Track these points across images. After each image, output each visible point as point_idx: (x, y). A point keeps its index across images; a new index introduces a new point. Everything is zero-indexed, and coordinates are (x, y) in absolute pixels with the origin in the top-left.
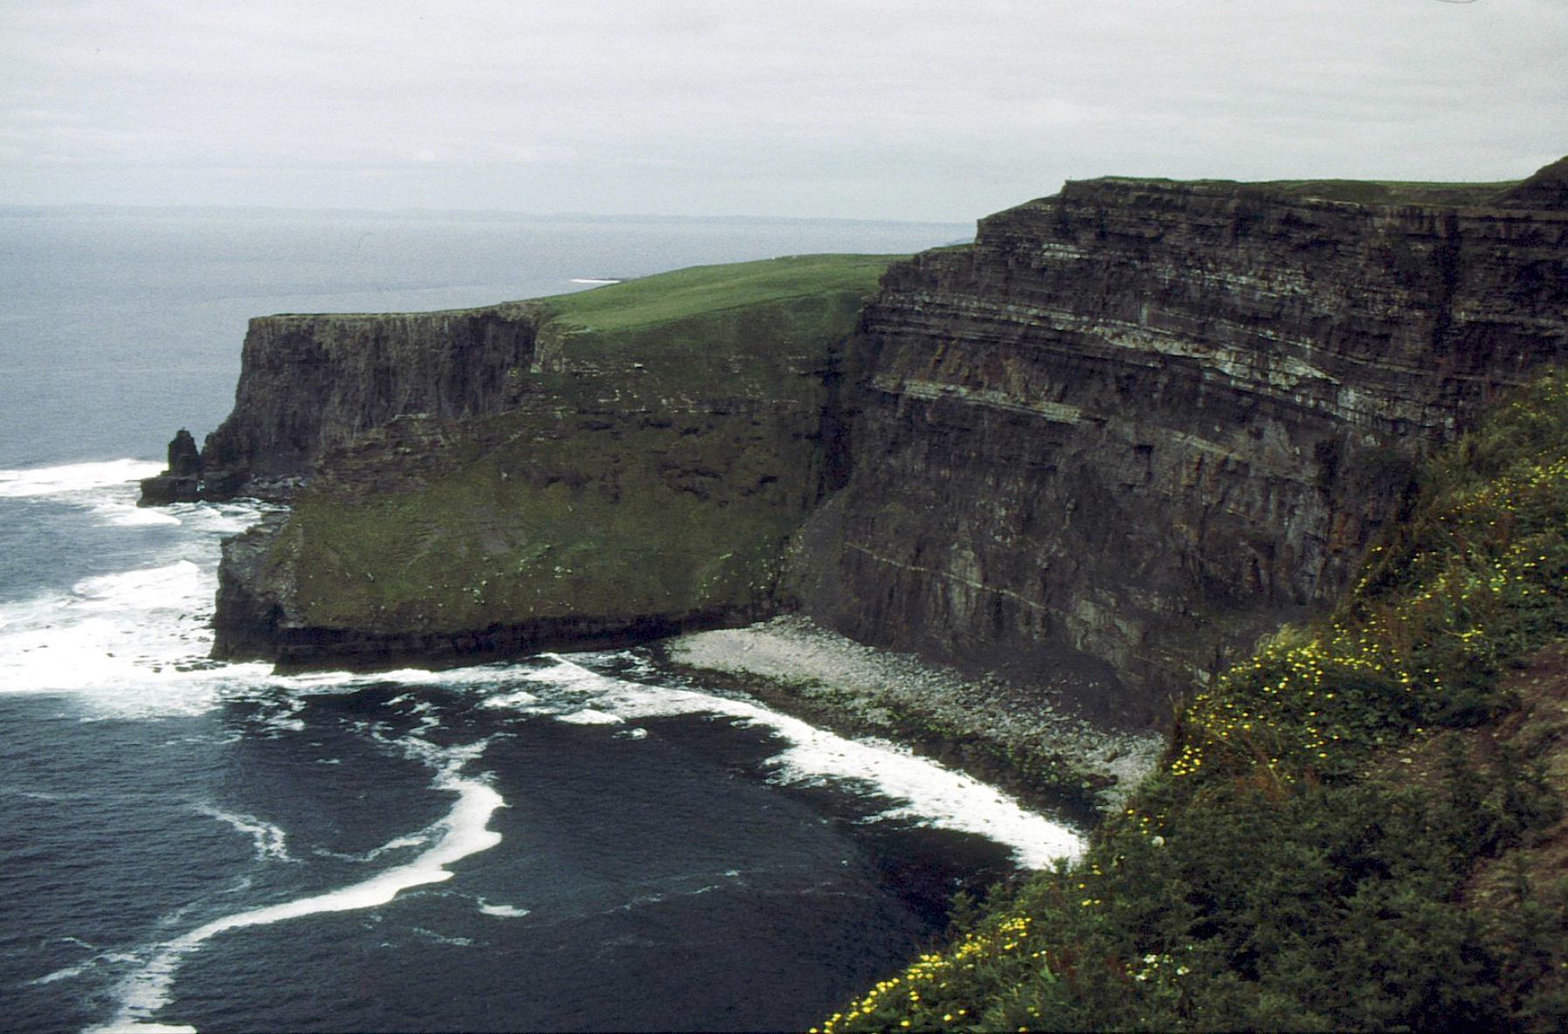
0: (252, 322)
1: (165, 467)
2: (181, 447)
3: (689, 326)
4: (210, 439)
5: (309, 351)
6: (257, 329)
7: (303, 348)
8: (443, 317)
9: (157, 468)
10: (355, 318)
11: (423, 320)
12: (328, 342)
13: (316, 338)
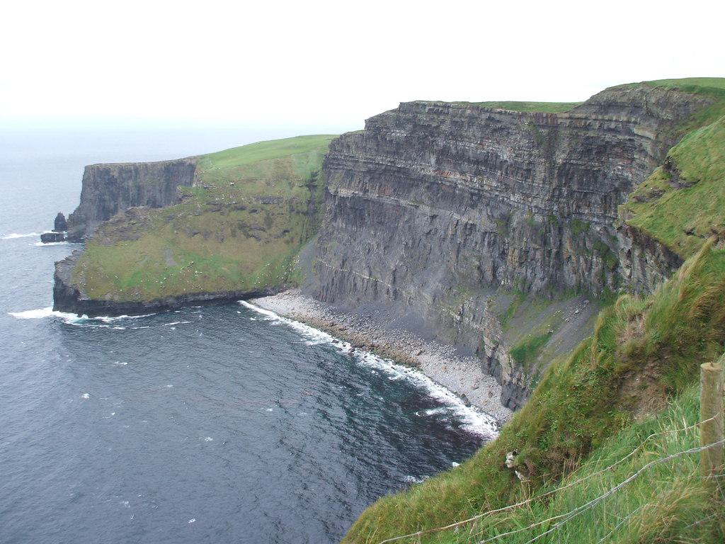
0: (86, 168)
2: (60, 223)
4: (70, 215)
6: (88, 169)
11: (154, 165)
12: (116, 175)
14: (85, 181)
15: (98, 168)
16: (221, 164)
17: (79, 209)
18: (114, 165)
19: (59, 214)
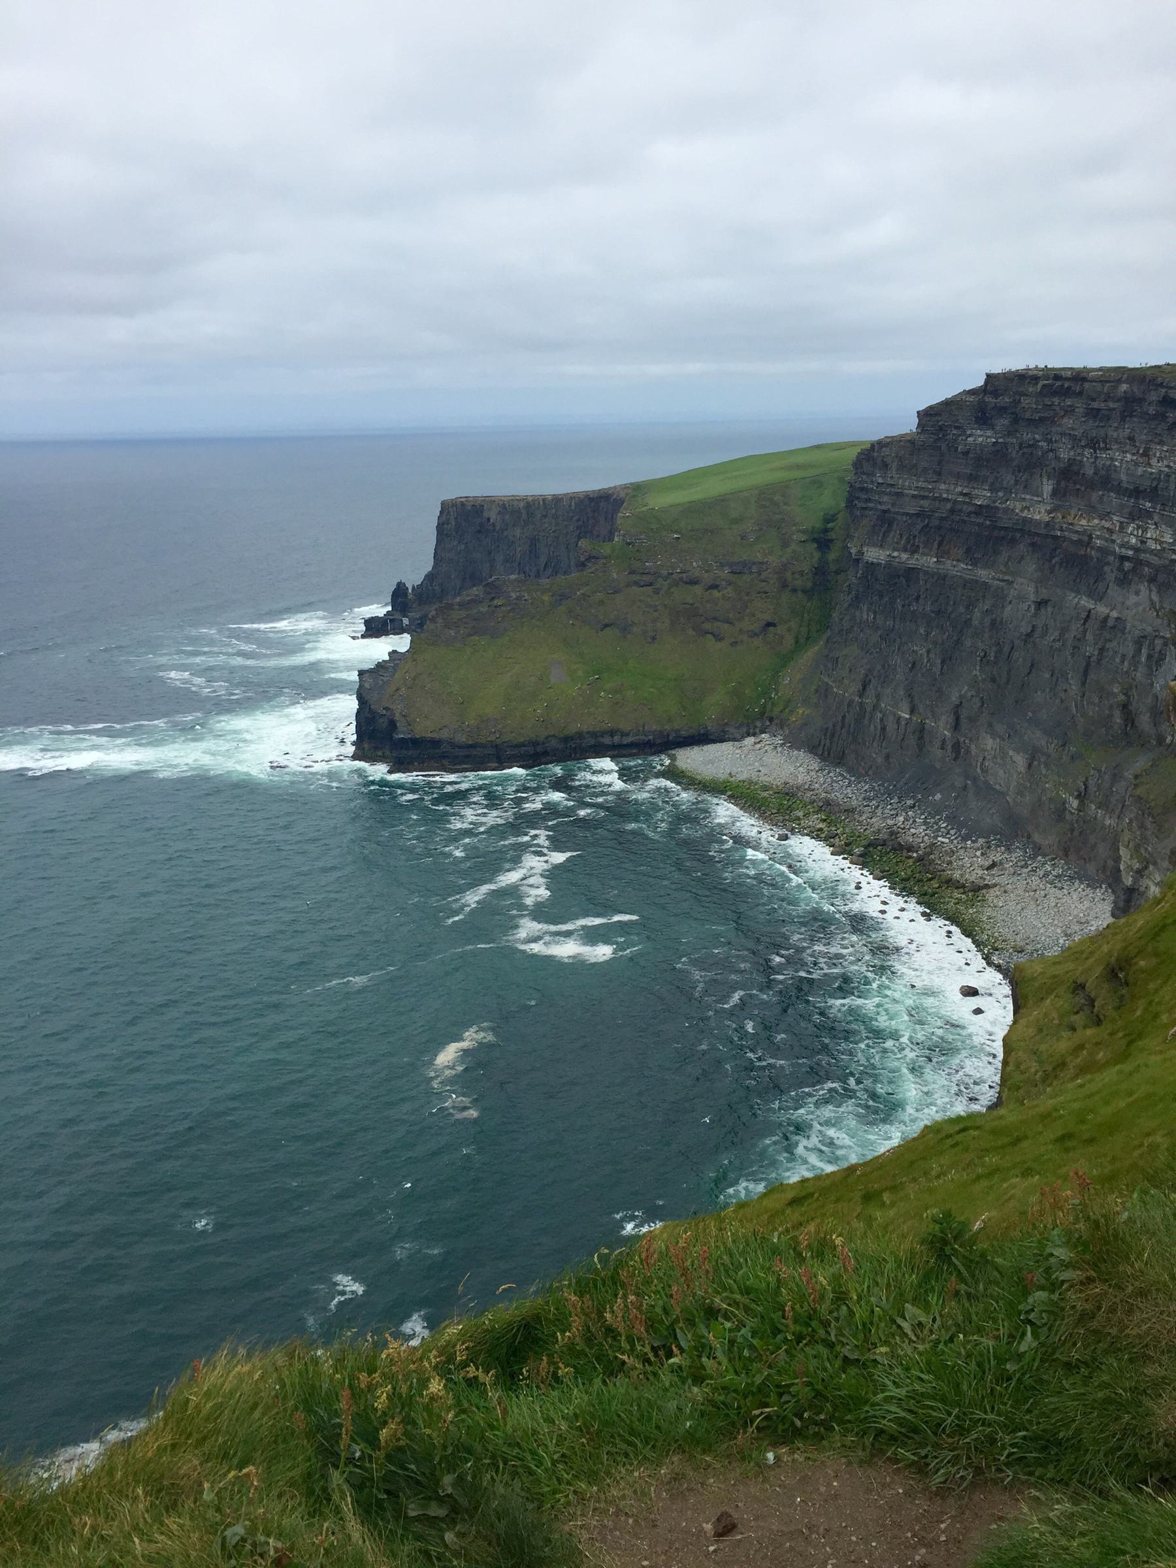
0: (443, 503)
1: (390, 608)
2: (399, 595)
3: (720, 502)
5: (481, 525)
6: (446, 507)
8: (572, 497)
9: (379, 610)
10: (515, 499)
11: (557, 499)
12: (493, 515)
13: (486, 514)
14: (440, 528)
15: (462, 504)
16: (658, 501)
17: (430, 577)
18: (490, 501)
19: (399, 584)
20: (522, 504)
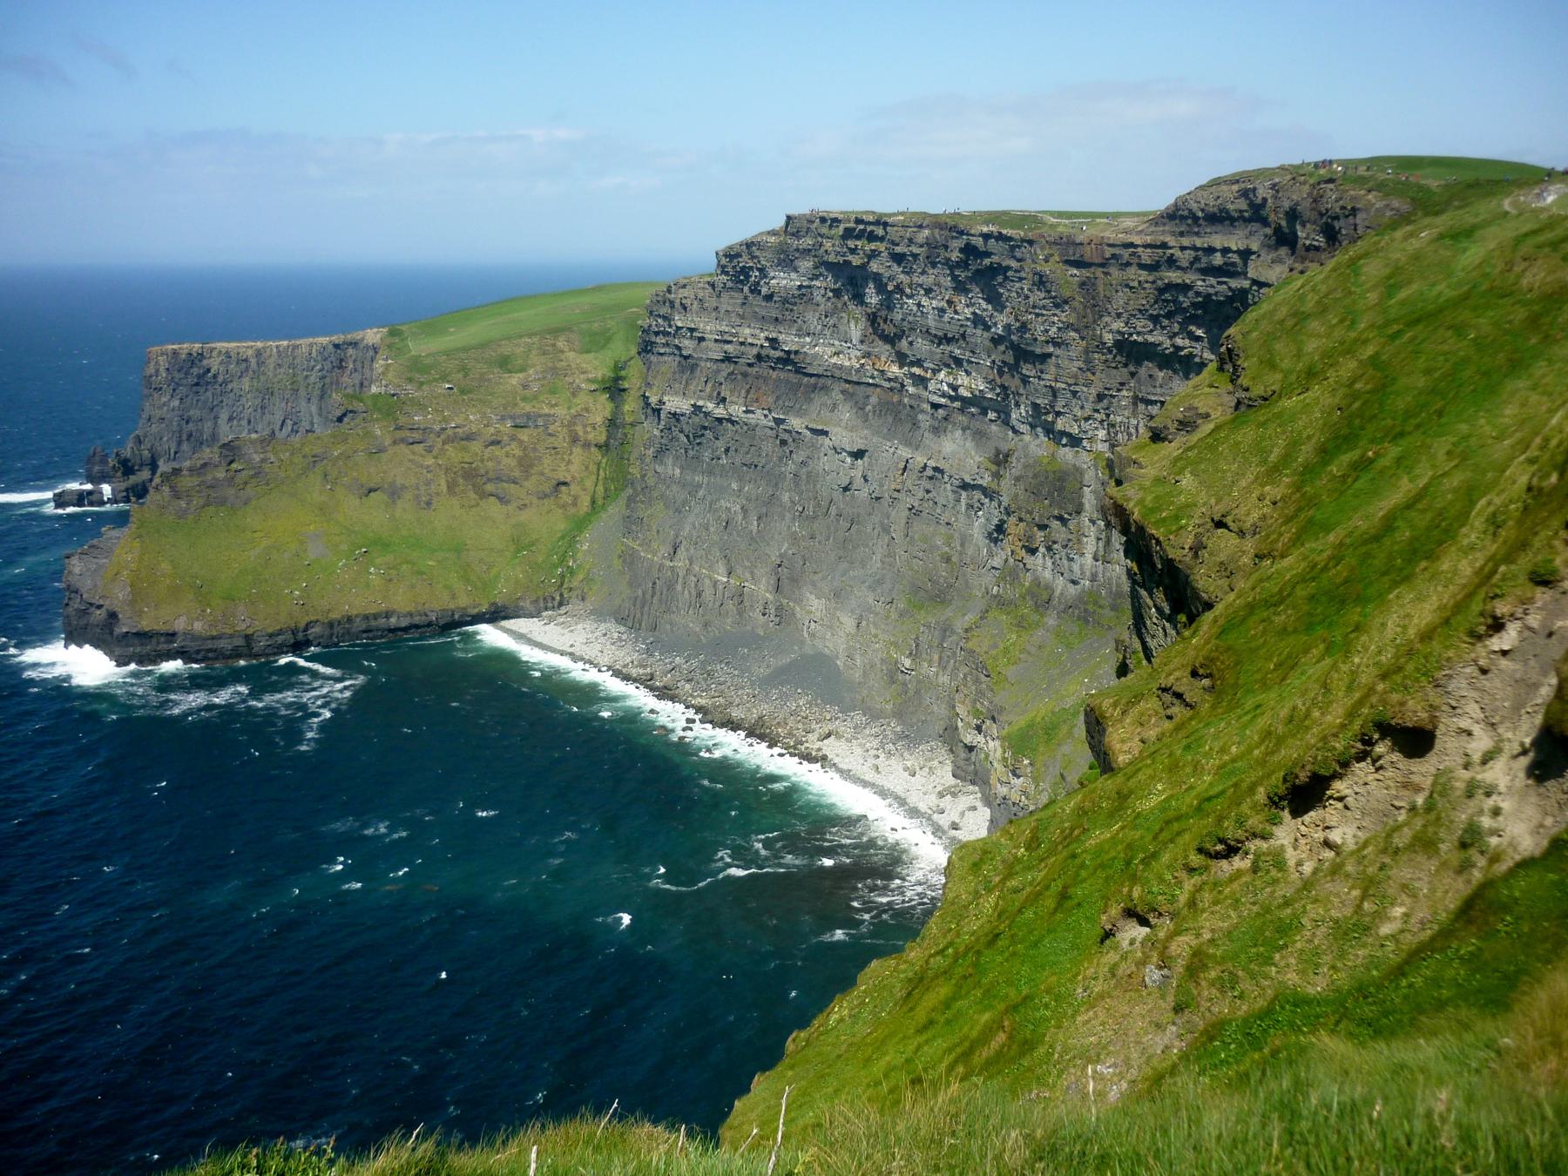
7: (195, 371)
20: (250, 352)
